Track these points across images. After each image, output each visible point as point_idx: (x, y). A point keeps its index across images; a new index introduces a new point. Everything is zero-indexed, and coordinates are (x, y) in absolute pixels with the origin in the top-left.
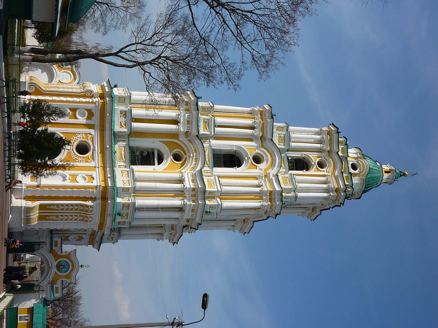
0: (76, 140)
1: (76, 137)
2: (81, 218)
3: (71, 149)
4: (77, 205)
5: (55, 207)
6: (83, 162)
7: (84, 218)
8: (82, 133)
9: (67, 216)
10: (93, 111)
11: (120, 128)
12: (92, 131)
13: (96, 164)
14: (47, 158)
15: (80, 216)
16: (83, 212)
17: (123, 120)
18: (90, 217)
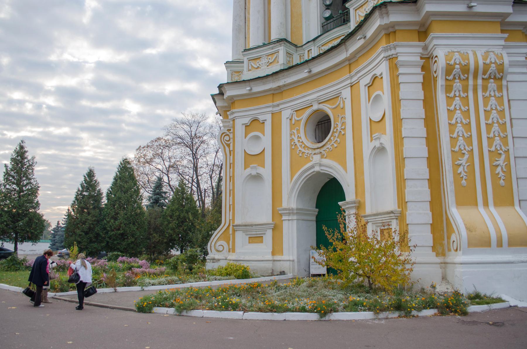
0: (303, 145)
1: (298, 144)
2: (492, 85)
3: (321, 153)
4: (450, 100)
5: (463, 161)
6: (345, 118)
7: (490, 77)
8: (291, 134)
9: (489, 126)
10: (247, 120)
11: (278, 62)
12: (286, 114)
13: (345, 87)
14: (339, 203)
15: (485, 89)
16: (471, 82)
17: (264, 61)
18: (485, 58)
